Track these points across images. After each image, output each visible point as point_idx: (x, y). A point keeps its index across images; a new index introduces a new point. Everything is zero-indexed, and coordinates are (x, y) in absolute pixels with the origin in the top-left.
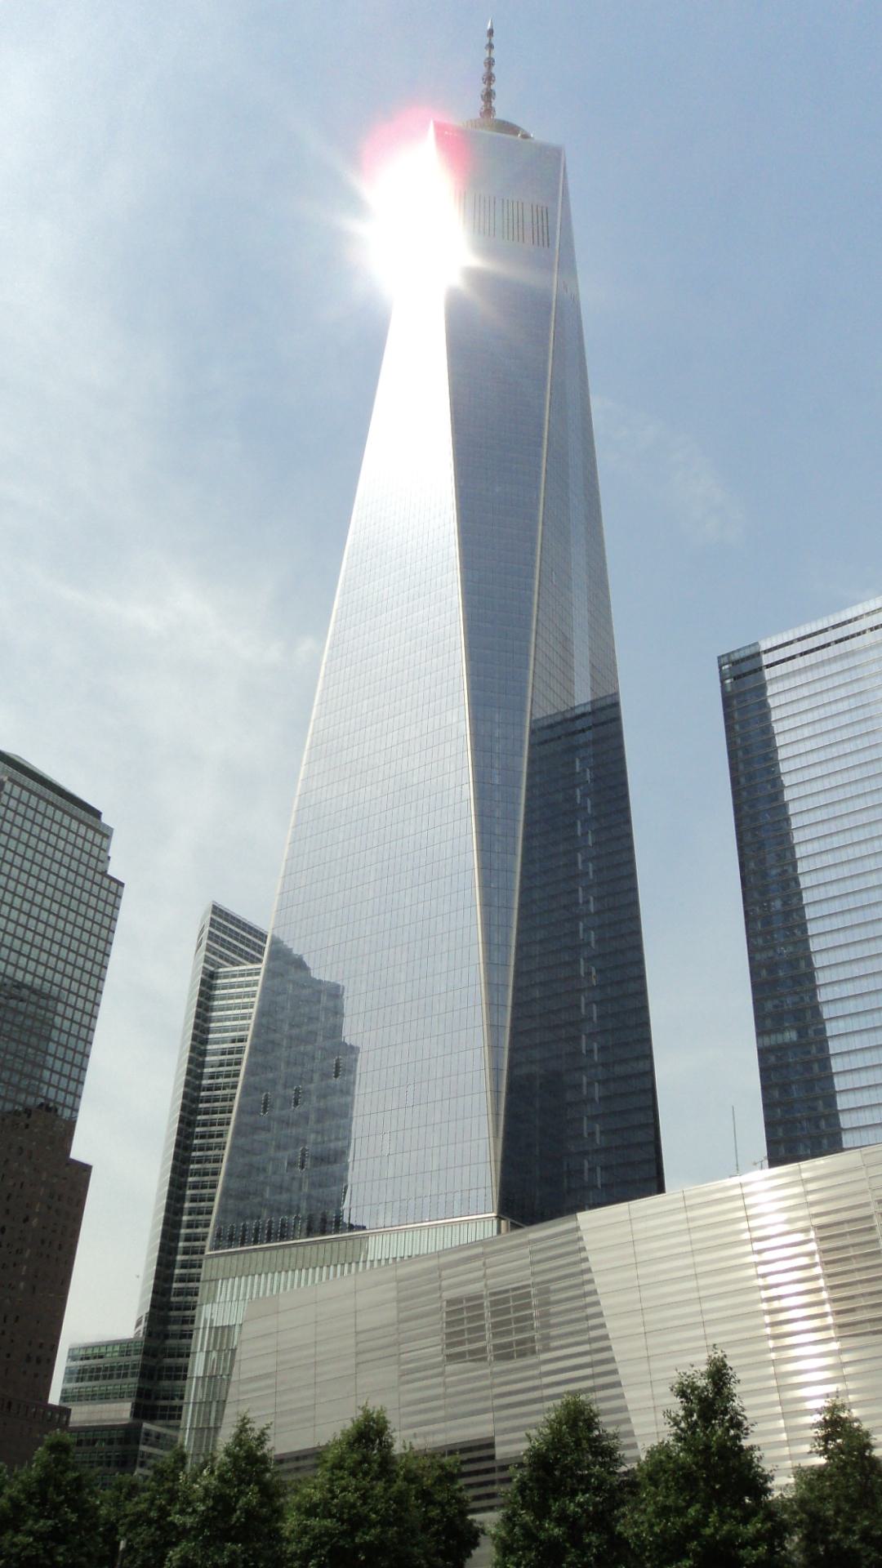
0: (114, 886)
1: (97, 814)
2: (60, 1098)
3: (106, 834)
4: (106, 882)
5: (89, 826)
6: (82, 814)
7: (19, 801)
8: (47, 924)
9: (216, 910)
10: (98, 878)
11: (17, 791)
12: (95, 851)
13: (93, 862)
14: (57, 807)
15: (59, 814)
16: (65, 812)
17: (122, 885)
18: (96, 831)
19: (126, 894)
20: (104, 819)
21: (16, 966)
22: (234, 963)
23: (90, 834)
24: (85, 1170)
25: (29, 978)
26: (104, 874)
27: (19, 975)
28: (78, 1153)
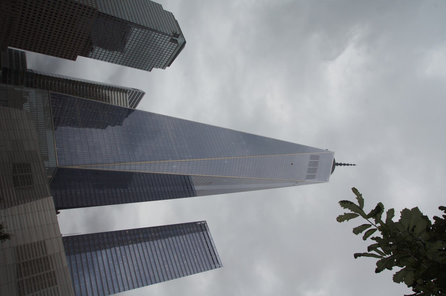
0: (150, 69)
1: (169, 66)
2: (94, 54)
3: (164, 68)
4: (151, 67)
5: (166, 64)
6: (169, 62)
7: (173, 47)
8: (140, 52)
9: (143, 94)
10: (152, 66)
11: (175, 47)
12: (159, 65)
13: (156, 64)
14: (171, 56)
15: (169, 56)
16: (169, 58)
17: (150, 71)
18: (164, 66)
19: (148, 72)
20: (167, 67)
21: (129, 45)
22: (129, 98)
23: (163, 64)
24: (74, 59)
25: (127, 47)
26: (153, 67)
27: (127, 45)
28: (79, 58)
